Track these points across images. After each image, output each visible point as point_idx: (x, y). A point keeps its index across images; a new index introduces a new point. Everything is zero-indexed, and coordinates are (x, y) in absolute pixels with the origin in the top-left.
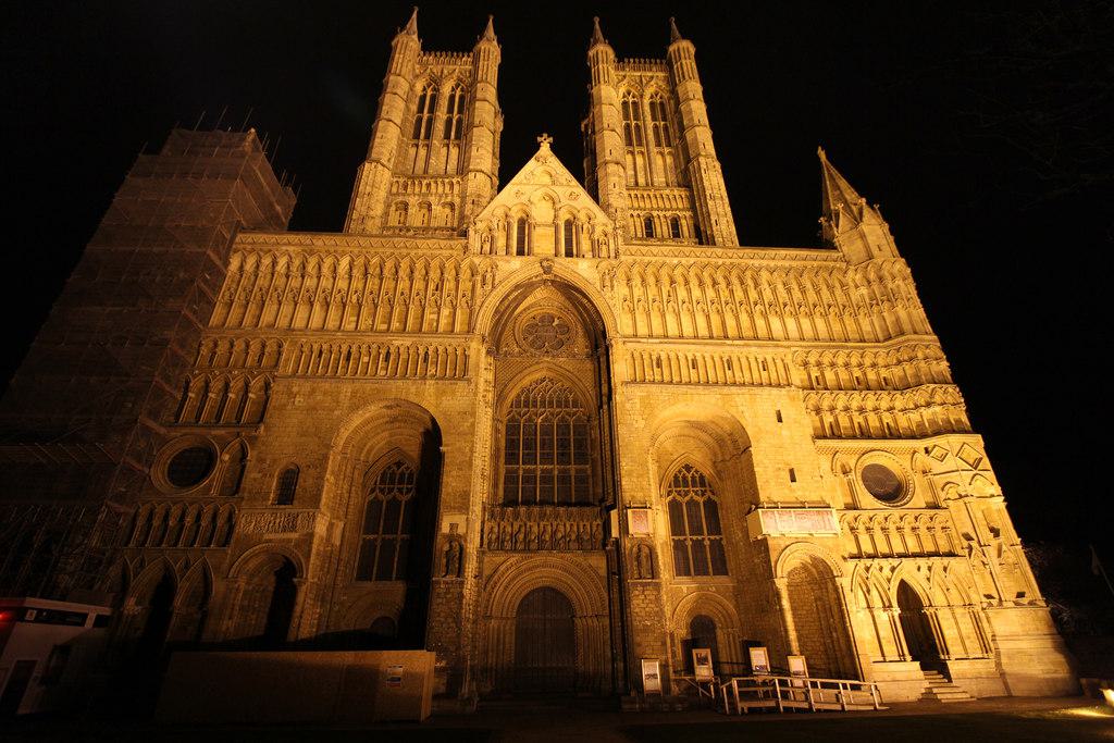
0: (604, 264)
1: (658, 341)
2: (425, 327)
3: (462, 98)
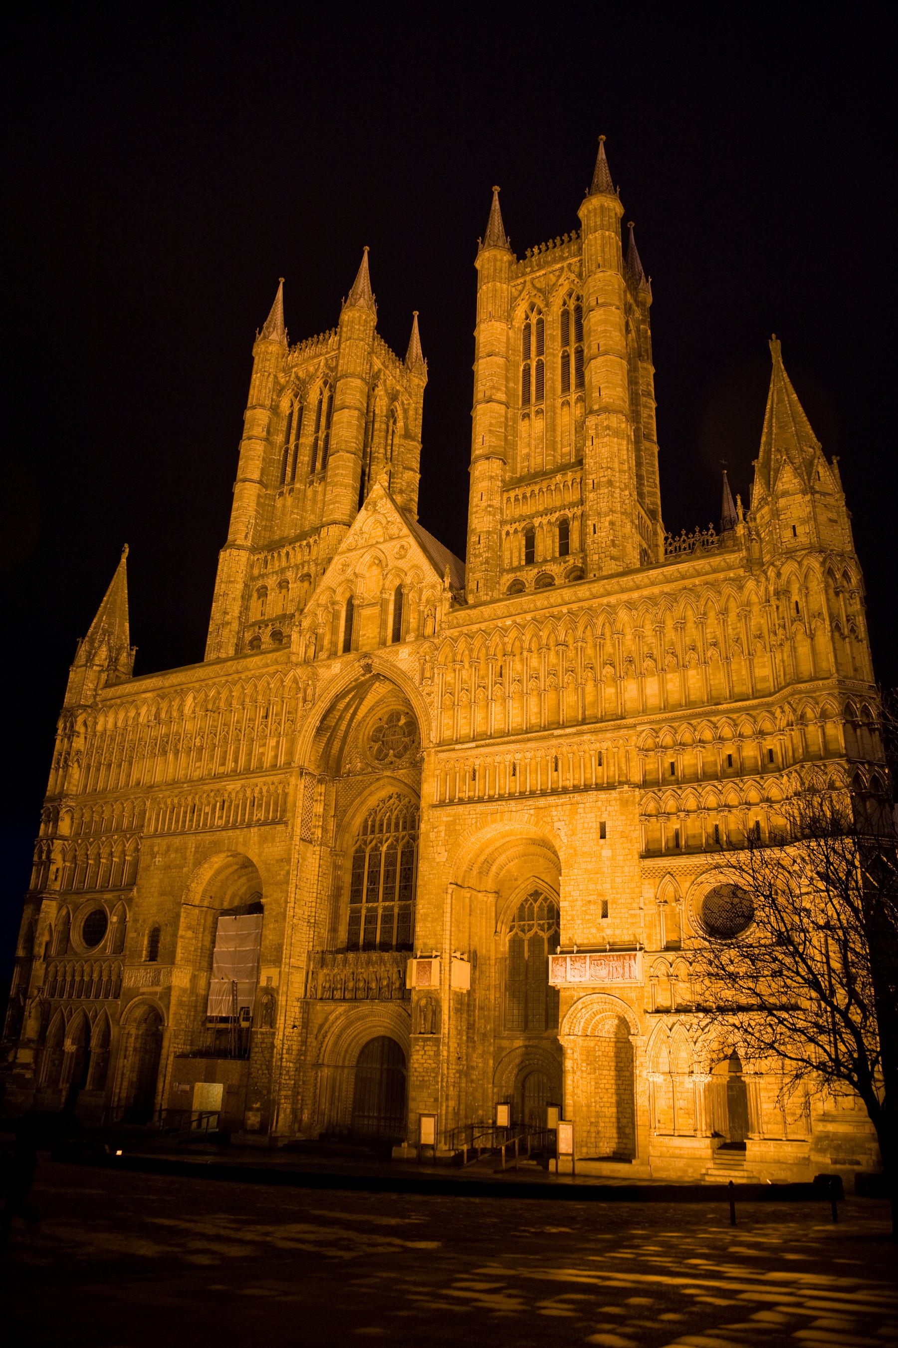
0: (427, 645)
1: (473, 744)
3: (331, 398)
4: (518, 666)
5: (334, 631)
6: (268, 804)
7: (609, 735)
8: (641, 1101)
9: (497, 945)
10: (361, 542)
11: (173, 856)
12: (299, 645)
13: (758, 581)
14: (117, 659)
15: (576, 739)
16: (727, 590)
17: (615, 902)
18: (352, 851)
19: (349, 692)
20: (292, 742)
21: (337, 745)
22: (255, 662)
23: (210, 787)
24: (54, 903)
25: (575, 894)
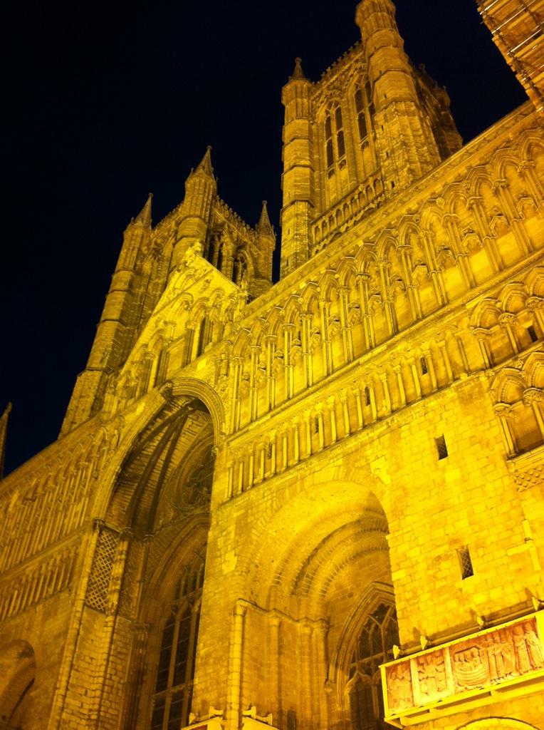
7: (429, 331)
15: (387, 355)
17: (480, 545)
25: (414, 553)
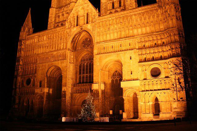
0: (94, 24)
2: (59, 49)
4: (112, 27)
5: (74, 22)
6: (62, 56)
7: (131, 40)
8: (139, 108)
9: (109, 81)
10: (79, 5)
11: (43, 67)
12: (67, 25)
13: (161, 10)
14: (29, 30)
16: (154, 11)
18: (79, 65)
19: (78, 34)
20: (67, 44)
21: (75, 44)
22: (58, 29)
23: (50, 53)
24: (20, 78)
25: (125, 70)
